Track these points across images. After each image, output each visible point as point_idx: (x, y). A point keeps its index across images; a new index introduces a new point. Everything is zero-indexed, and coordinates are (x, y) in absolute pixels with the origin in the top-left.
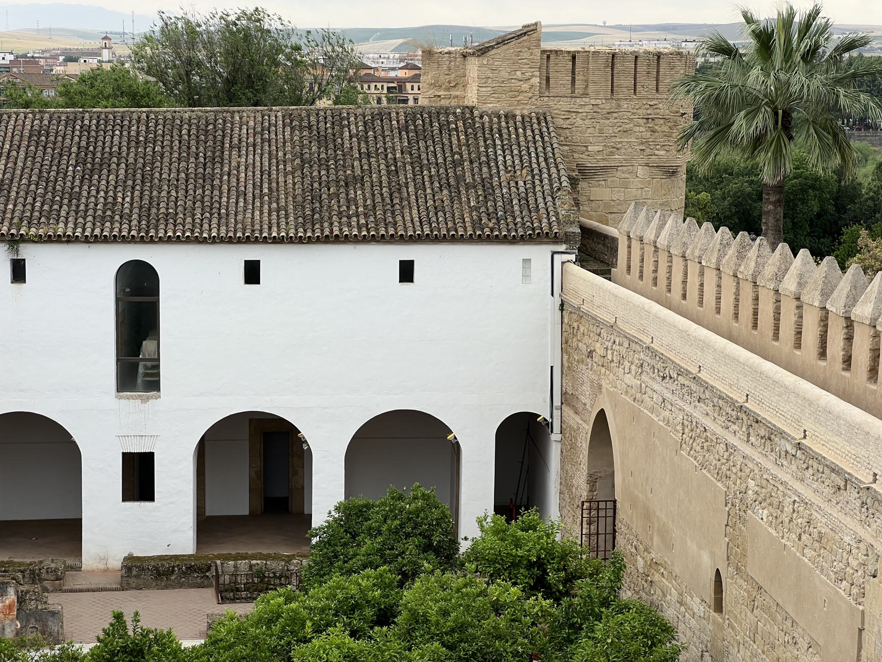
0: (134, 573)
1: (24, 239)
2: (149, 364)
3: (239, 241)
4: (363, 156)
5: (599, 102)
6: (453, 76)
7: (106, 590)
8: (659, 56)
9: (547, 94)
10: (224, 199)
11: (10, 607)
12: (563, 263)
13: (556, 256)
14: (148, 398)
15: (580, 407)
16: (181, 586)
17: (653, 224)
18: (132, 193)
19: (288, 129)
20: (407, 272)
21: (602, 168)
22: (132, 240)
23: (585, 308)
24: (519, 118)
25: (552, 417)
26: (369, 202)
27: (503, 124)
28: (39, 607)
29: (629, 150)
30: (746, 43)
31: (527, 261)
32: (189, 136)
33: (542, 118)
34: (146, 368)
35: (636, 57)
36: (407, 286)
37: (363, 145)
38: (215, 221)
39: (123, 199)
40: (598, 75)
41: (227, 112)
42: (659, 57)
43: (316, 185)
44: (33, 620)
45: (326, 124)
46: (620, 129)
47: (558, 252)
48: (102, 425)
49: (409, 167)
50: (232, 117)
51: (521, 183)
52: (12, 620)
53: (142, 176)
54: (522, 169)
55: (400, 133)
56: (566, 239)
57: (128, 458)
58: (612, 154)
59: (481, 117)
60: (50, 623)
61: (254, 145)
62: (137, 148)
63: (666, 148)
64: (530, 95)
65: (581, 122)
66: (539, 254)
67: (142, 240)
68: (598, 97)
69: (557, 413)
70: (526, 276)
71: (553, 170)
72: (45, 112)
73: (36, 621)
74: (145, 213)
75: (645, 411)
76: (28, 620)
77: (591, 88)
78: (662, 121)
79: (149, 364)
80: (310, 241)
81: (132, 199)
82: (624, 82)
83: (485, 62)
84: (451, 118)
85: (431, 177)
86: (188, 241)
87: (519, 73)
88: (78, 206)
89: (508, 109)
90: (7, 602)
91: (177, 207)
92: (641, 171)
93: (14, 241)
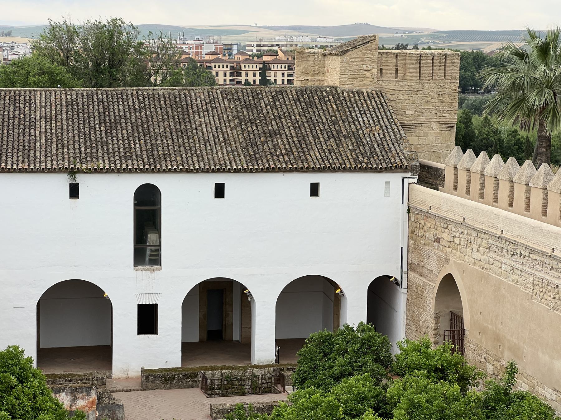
0: (151, 379)
1: (79, 171)
2: (153, 248)
3: (213, 171)
4: (276, 117)
5: (412, 84)
6: (317, 67)
7: (133, 390)
8: (446, 56)
9: (381, 79)
10: (197, 145)
11: (92, 403)
12: (409, 184)
13: (405, 180)
14: (154, 270)
15: (425, 272)
17: (454, 160)
18: (139, 141)
19: (226, 100)
20: (315, 190)
21: (413, 124)
22: (147, 171)
23: (433, 211)
24: (365, 94)
25: (402, 278)
26: (287, 147)
27: (357, 97)
28: (111, 402)
29: (429, 113)
30: (531, 50)
31: (387, 183)
32: (166, 105)
33: (380, 94)
34: (151, 251)
35: (433, 56)
36: (315, 198)
37: (275, 111)
38: (195, 159)
39: (135, 145)
40: (412, 67)
41: (186, 90)
42: (446, 56)
43: (252, 136)
44: (106, 411)
45: (248, 97)
46: (424, 100)
47: (406, 178)
48: (125, 288)
49: (306, 125)
50: (190, 93)
51: (376, 135)
52: (94, 411)
53: (142, 130)
54: (375, 126)
55: (296, 104)
56: (411, 169)
58: (419, 116)
59: (343, 93)
60: (117, 412)
61: (208, 111)
62: (135, 113)
63: (449, 112)
64: (372, 79)
65: (402, 96)
66: (395, 179)
67: (153, 171)
68: (411, 81)
69: (405, 276)
71: (394, 126)
72: (73, 90)
73: (109, 411)
74: (151, 153)
75: (493, 275)
76: (103, 411)
77: (408, 75)
78: (447, 96)
79: (153, 248)
80: (257, 171)
81: (140, 145)
82: (427, 71)
83: (345, 59)
84: (325, 94)
85: (321, 131)
86: (181, 171)
87: (365, 66)
88: (108, 150)
89: (358, 88)
90: (91, 400)
91: (169, 150)
92: (435, 126)
93: (73, 172)
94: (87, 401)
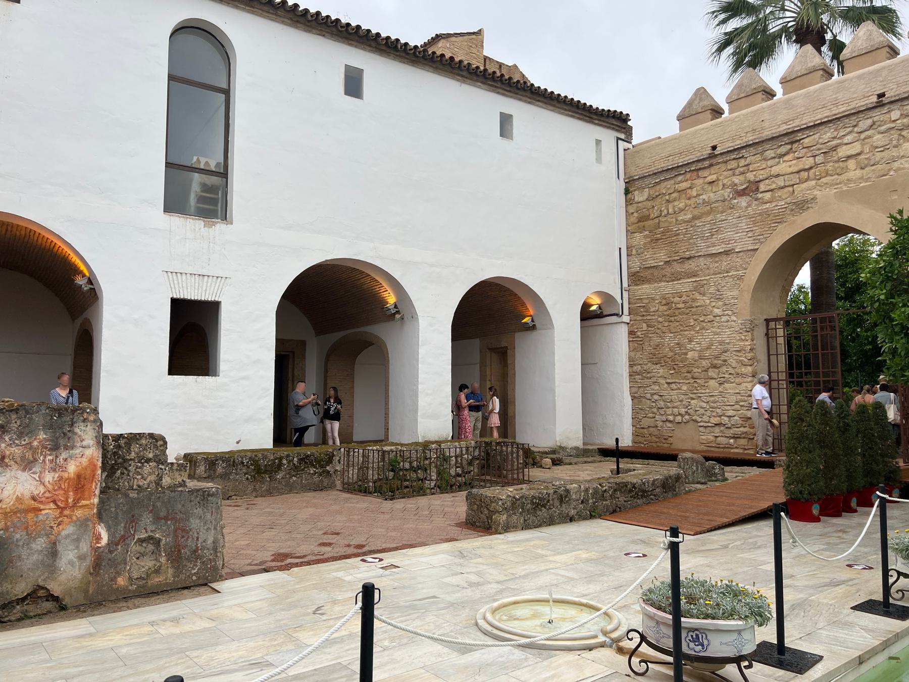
0: (220, 470)
11: (80, 483)
16: (291, 489)
28: (166, 481)
31: (598, 142)
44: (147, 519)
52: (83, 524)
57: (179, 306)
60: (194, 523)
69: (625, 295)
70: (599, 160)
73: (157, 519)
76: (133, 520)
90: (72, 468)
94: (49, 477)
